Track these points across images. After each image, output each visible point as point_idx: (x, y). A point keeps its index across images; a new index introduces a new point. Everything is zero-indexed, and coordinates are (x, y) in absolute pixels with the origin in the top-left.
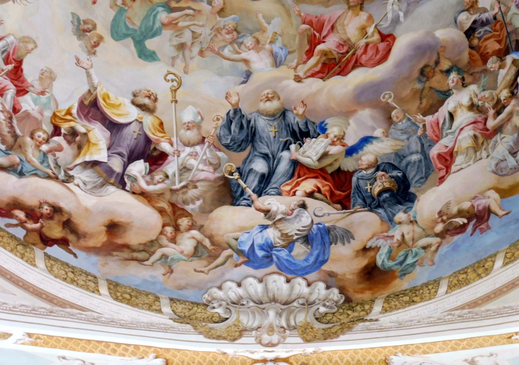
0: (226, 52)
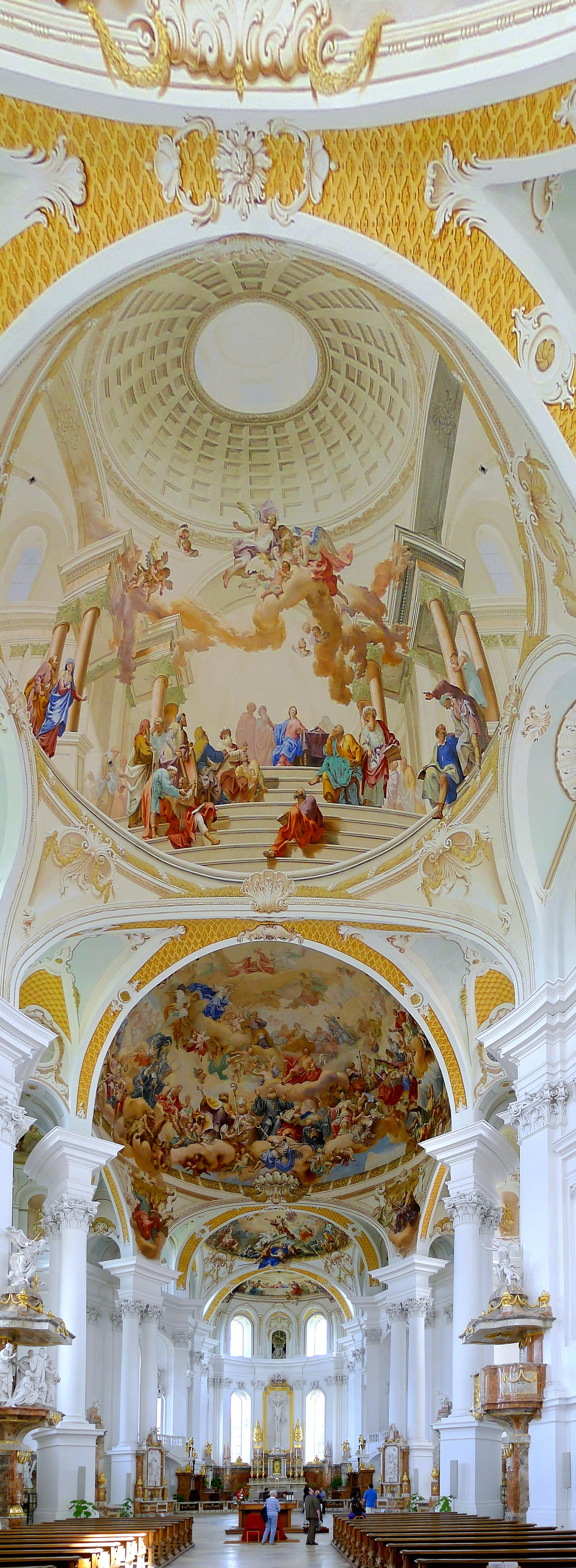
0: (254, 1072)
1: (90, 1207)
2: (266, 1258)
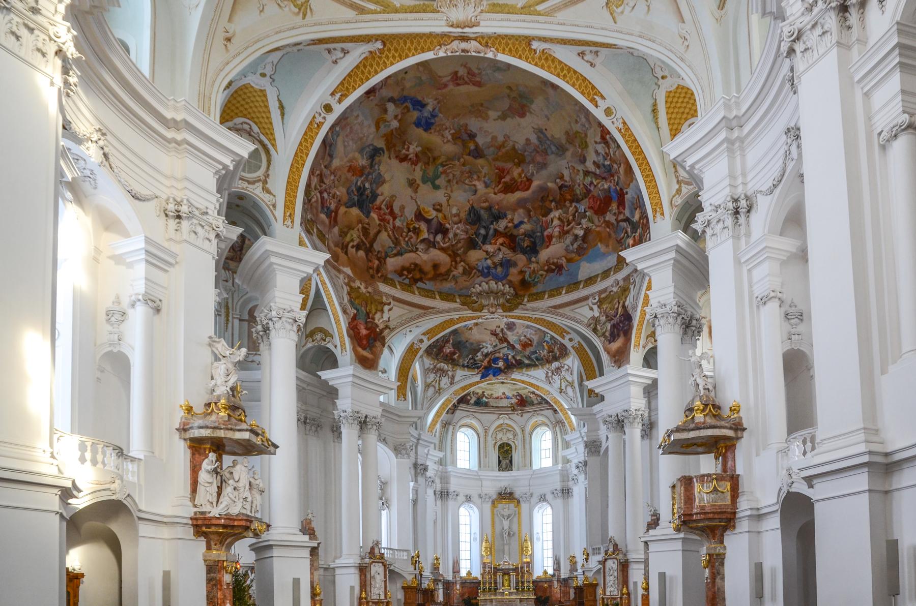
1: (297, 316)
2: (487, 368)
